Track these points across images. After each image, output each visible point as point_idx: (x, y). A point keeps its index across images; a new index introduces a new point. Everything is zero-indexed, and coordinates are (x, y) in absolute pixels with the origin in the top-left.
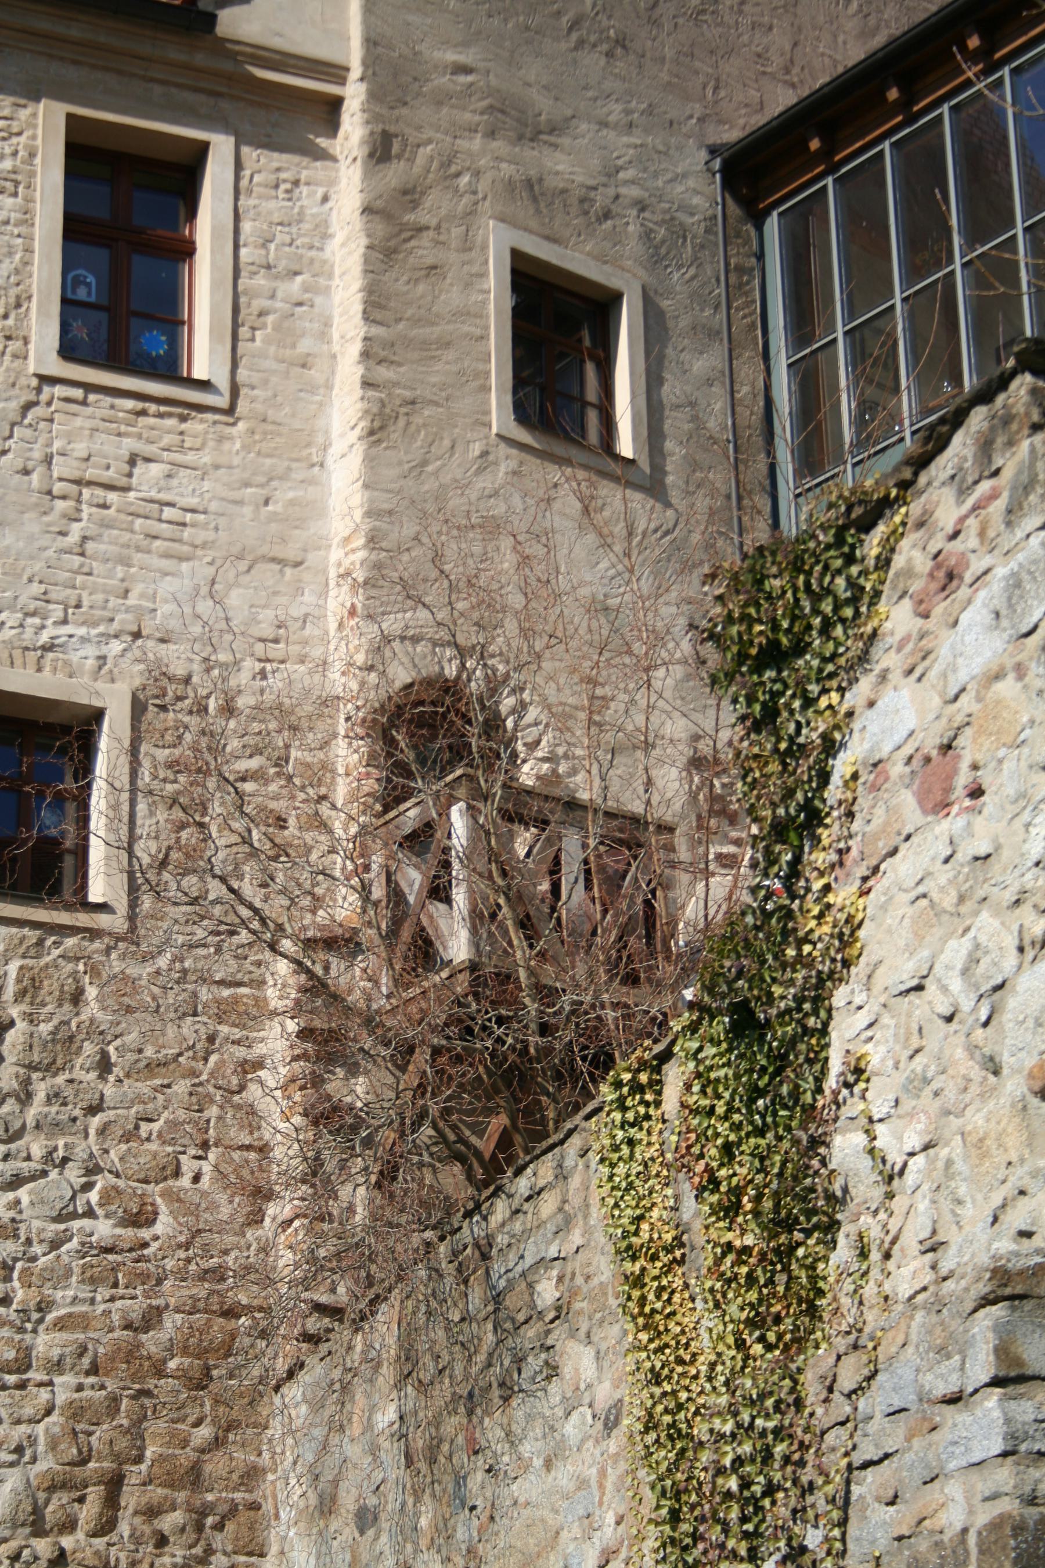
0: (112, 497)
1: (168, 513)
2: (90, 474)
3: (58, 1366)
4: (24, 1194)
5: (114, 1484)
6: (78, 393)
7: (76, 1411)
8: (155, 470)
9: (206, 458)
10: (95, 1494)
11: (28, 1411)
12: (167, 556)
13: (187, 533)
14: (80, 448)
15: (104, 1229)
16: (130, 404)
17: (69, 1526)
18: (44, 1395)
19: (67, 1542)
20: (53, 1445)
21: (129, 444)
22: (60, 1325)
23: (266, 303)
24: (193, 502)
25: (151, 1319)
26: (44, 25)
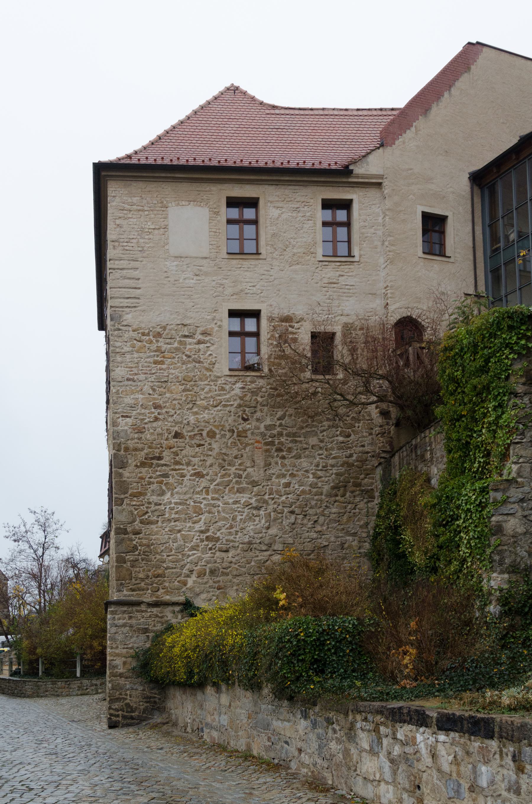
0: (335, 285)
1: (347, 287)
2: (331, 281)
3: (333, 466)
4: (325, 433)
5: (345, 486)
6: (327, 263)
7: (337, 474)
8: (343, 278)
9: (354, 274)
10: (342, 489)
11: (328, 475)
12: (347, 297)
13: (351, 291)
14: (328, 275)
15: (341, 439)
16: (338, 264)
17: (337, 495)
18: (331, 472)
19: (337, 498)
20: (333, 481)
21: (338, 273)
22: (334, 458)
23: (366, 235)
24: (352, 284)
25: (351, 456)
26: (316, 179)
